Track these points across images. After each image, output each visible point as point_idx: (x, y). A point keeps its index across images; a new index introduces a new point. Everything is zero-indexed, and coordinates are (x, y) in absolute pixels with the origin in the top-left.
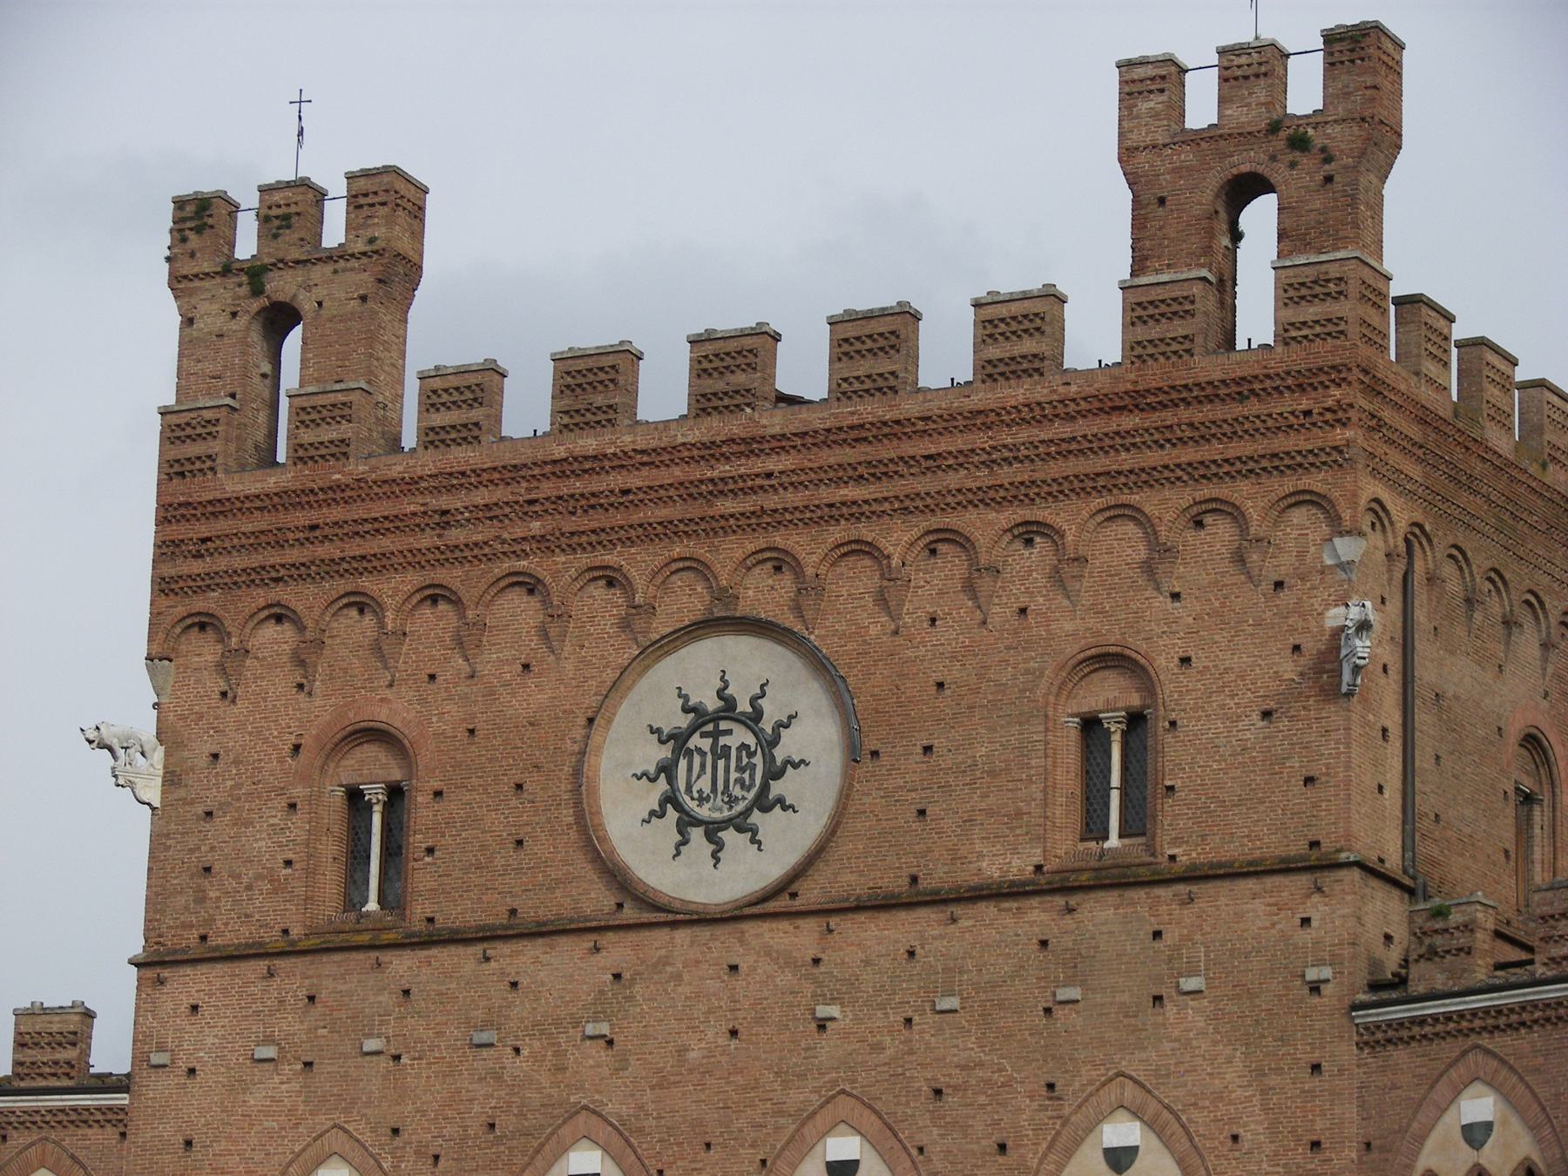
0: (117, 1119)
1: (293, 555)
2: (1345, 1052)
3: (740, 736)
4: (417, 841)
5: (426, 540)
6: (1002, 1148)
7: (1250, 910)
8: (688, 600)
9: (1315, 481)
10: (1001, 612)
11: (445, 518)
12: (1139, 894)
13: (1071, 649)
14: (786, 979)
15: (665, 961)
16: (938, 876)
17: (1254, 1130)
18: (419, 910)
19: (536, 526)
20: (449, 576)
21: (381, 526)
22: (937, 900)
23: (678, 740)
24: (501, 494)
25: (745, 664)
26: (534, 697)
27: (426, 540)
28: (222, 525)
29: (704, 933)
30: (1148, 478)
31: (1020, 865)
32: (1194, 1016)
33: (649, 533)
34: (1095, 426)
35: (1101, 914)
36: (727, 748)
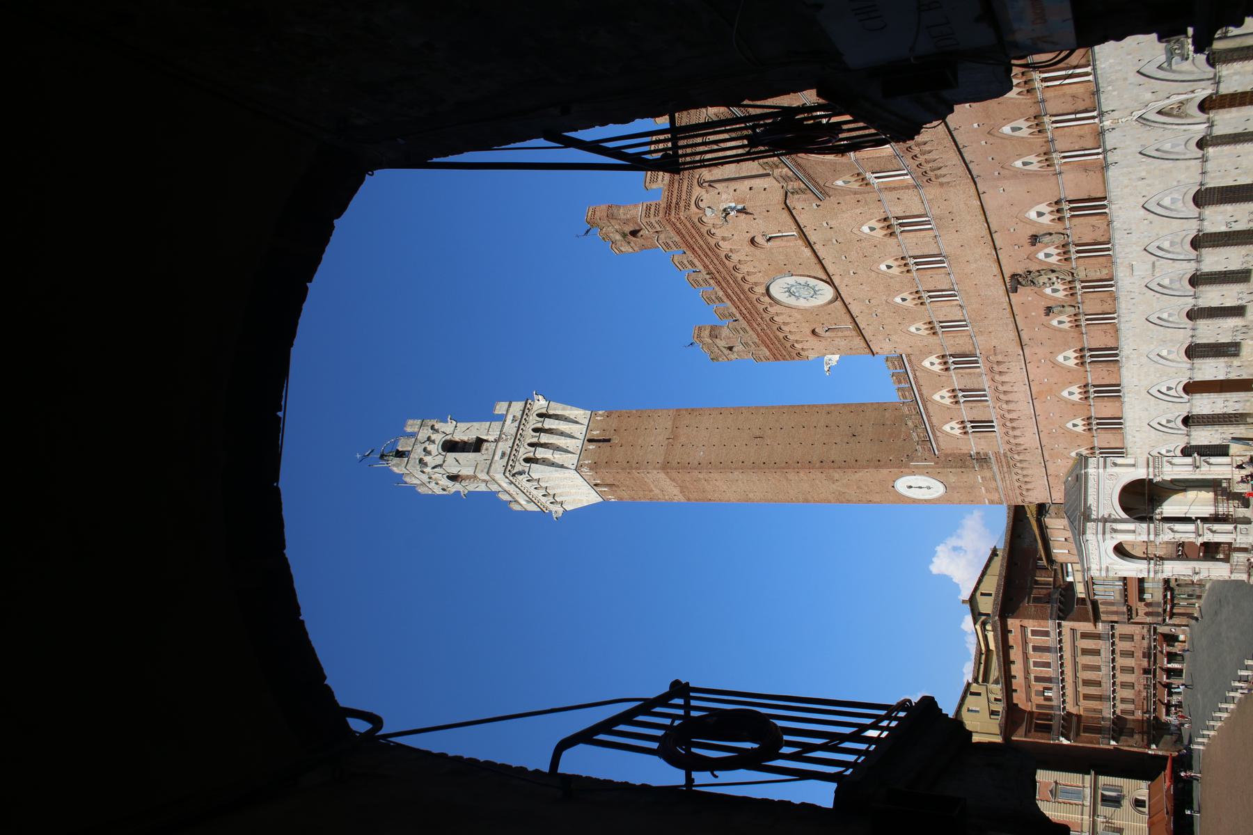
0: (908, 356)
3: (793, 289)
8: (767, 299)
10: (748, 258)
13: (753, 248)
16: (814, 260)
23: (798, 298)
30: (708, 244)
31: (807, 252)
35: (812, 239)
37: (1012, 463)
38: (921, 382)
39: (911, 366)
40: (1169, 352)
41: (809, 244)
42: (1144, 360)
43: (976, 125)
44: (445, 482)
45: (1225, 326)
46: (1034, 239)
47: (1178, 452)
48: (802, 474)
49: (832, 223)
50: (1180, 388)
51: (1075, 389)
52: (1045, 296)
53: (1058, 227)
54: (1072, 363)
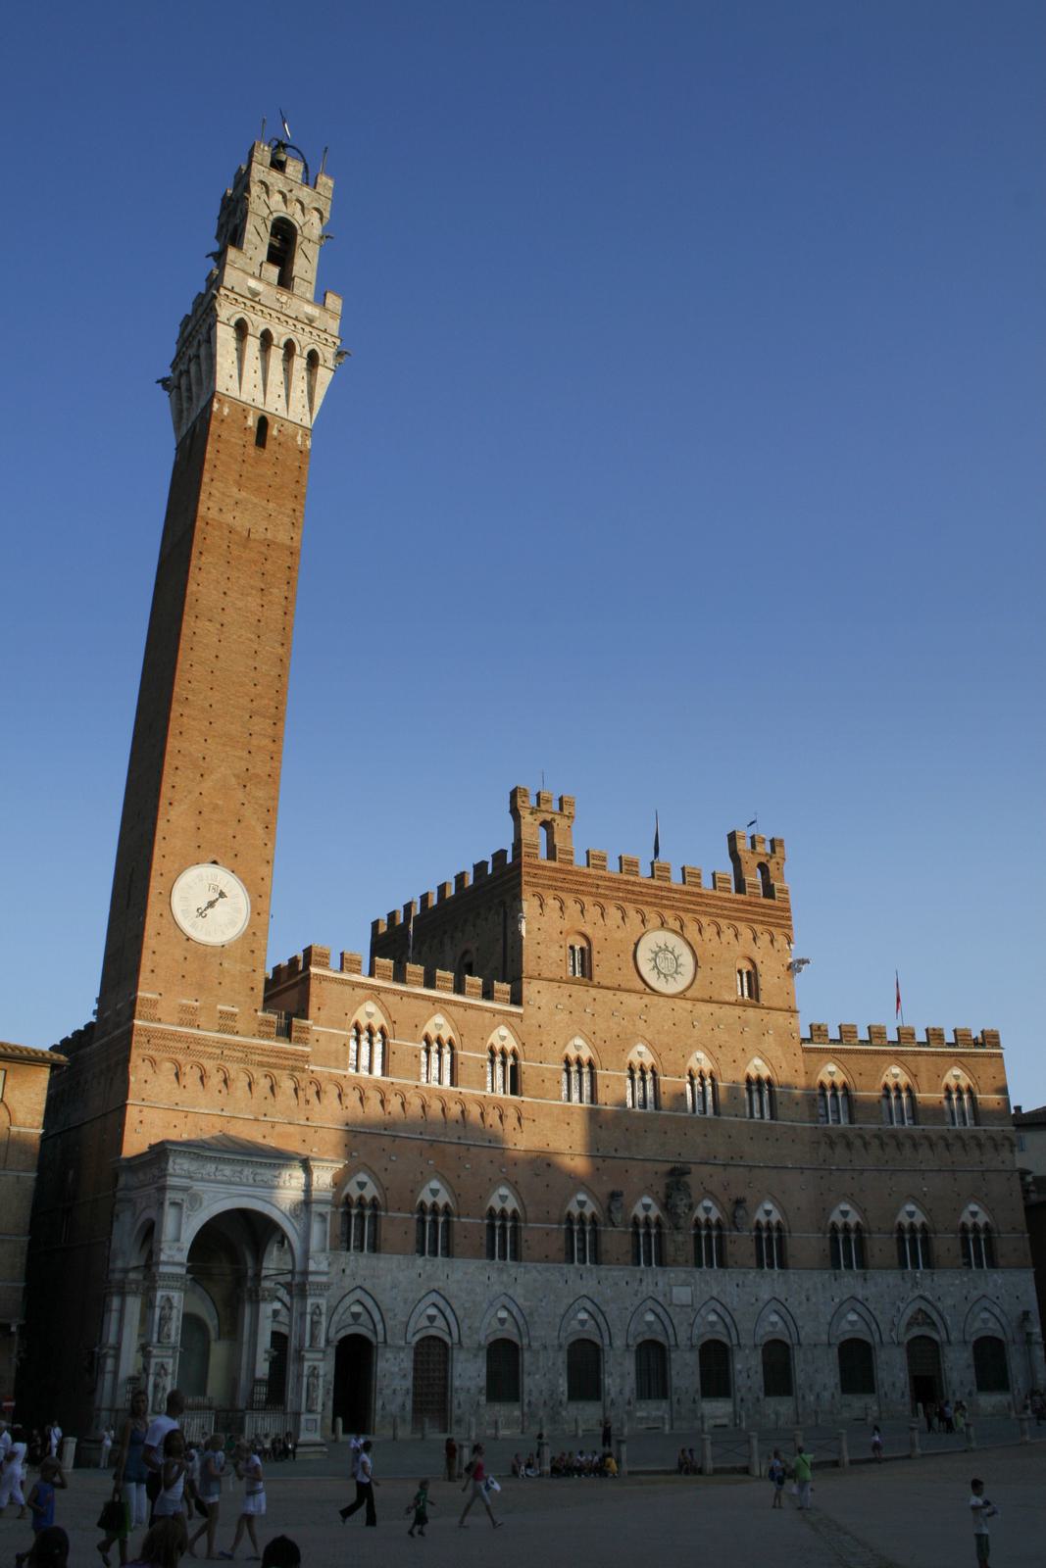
0: (520, 1016)
1: (559, 884)
2: (799, 1052)
3: (670, 956)
4: (594, 963)
5: (594, 890)
6: (734, 1061)
7: (780, 1018)
9: (786, 931)
11: (598, 886)
12: (757, 1010)
14: (685, 1014)
15: (656, 1005)
17: (784, 1065)
18: (596, 980)
19: (621, 895)
20: (602, 901)
21: (582, 884)
22: (717, 1002)
24: (611, 884)
25: (673, 940)
26: (619, 935)
27: (594, 890)
28: (540, 872)
29: (666, 999)
31: (733, 999)
32: (771, 1039)
33: (647, 903)
34: (741, 907)
35: (751, 1012)
36: (666, 959)
37: (275, 1072)
38: (470, 1012)
39: (500, 1012)
40: (502, 1321)
41: (744, 1005)
42: (497, 1288)
43: (925, 1189)
44: (279, 209)
45: (561, 1381)
46: (739, 1203)
47: (278, 1328)
48: (266, 742)
49: (769, 1039)
50: (433, 1332)
51: (443, 1199)
52: (640, 1195)
53: (752, 1225)
54: (495, 1202)
